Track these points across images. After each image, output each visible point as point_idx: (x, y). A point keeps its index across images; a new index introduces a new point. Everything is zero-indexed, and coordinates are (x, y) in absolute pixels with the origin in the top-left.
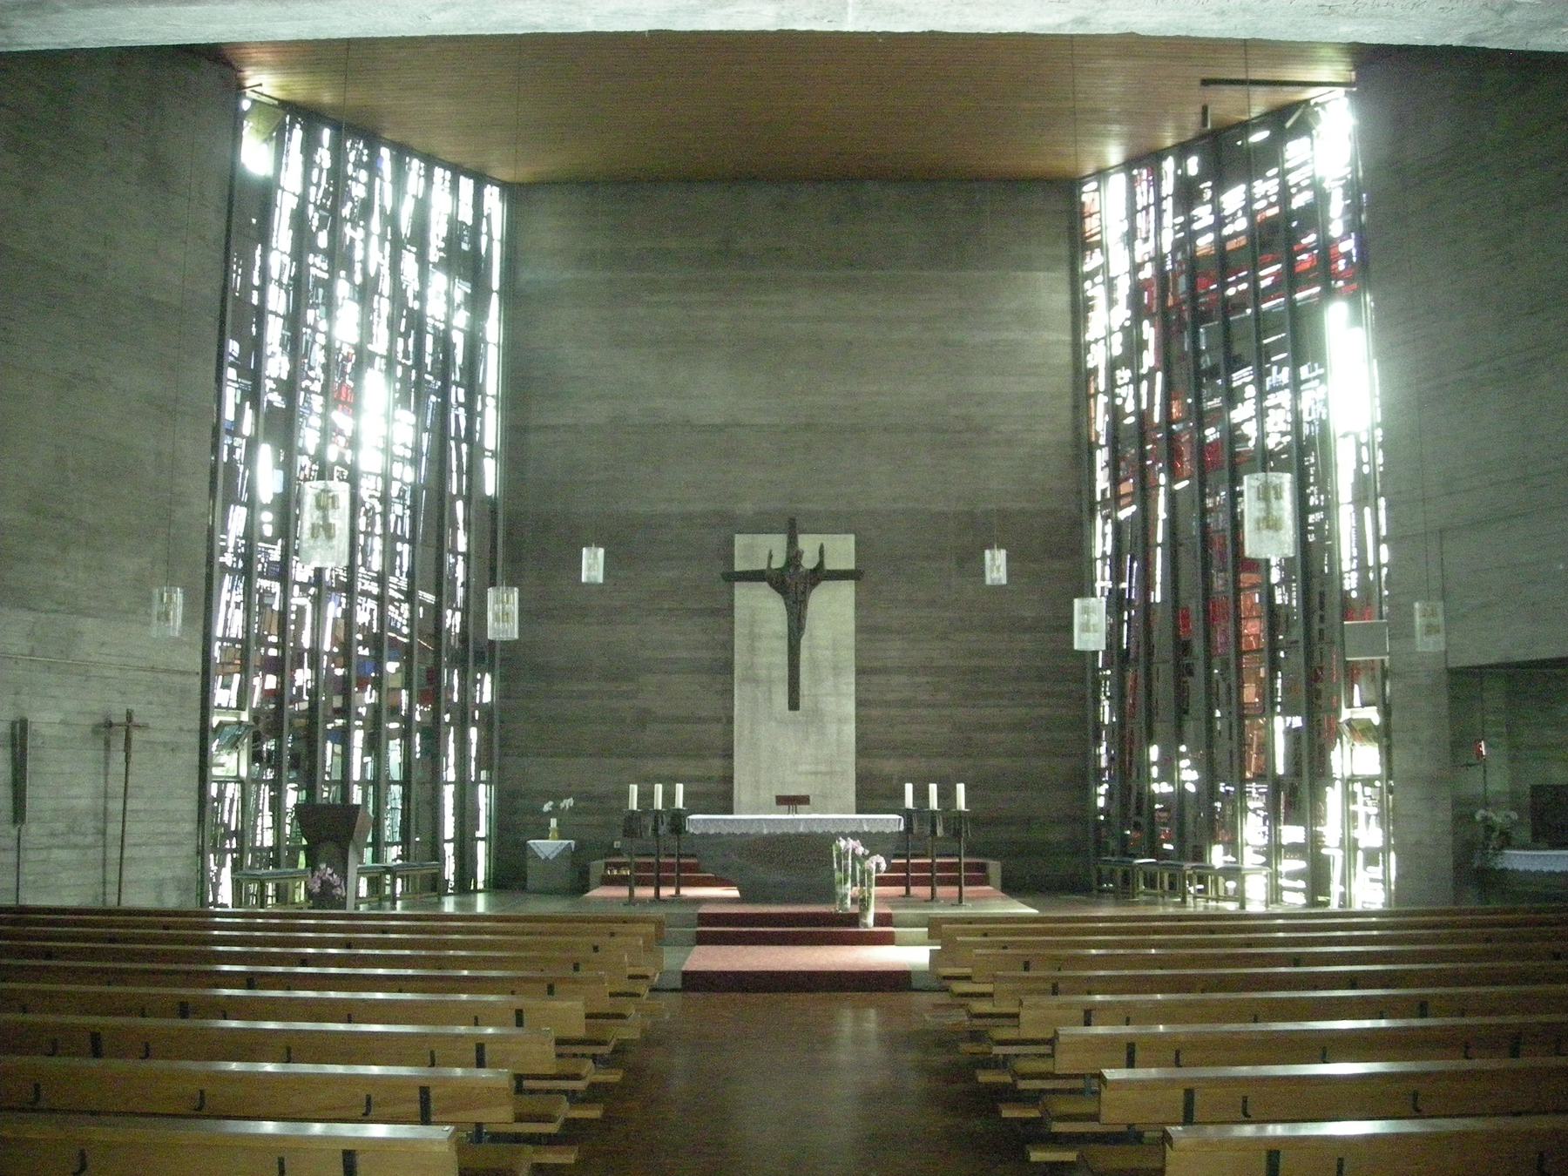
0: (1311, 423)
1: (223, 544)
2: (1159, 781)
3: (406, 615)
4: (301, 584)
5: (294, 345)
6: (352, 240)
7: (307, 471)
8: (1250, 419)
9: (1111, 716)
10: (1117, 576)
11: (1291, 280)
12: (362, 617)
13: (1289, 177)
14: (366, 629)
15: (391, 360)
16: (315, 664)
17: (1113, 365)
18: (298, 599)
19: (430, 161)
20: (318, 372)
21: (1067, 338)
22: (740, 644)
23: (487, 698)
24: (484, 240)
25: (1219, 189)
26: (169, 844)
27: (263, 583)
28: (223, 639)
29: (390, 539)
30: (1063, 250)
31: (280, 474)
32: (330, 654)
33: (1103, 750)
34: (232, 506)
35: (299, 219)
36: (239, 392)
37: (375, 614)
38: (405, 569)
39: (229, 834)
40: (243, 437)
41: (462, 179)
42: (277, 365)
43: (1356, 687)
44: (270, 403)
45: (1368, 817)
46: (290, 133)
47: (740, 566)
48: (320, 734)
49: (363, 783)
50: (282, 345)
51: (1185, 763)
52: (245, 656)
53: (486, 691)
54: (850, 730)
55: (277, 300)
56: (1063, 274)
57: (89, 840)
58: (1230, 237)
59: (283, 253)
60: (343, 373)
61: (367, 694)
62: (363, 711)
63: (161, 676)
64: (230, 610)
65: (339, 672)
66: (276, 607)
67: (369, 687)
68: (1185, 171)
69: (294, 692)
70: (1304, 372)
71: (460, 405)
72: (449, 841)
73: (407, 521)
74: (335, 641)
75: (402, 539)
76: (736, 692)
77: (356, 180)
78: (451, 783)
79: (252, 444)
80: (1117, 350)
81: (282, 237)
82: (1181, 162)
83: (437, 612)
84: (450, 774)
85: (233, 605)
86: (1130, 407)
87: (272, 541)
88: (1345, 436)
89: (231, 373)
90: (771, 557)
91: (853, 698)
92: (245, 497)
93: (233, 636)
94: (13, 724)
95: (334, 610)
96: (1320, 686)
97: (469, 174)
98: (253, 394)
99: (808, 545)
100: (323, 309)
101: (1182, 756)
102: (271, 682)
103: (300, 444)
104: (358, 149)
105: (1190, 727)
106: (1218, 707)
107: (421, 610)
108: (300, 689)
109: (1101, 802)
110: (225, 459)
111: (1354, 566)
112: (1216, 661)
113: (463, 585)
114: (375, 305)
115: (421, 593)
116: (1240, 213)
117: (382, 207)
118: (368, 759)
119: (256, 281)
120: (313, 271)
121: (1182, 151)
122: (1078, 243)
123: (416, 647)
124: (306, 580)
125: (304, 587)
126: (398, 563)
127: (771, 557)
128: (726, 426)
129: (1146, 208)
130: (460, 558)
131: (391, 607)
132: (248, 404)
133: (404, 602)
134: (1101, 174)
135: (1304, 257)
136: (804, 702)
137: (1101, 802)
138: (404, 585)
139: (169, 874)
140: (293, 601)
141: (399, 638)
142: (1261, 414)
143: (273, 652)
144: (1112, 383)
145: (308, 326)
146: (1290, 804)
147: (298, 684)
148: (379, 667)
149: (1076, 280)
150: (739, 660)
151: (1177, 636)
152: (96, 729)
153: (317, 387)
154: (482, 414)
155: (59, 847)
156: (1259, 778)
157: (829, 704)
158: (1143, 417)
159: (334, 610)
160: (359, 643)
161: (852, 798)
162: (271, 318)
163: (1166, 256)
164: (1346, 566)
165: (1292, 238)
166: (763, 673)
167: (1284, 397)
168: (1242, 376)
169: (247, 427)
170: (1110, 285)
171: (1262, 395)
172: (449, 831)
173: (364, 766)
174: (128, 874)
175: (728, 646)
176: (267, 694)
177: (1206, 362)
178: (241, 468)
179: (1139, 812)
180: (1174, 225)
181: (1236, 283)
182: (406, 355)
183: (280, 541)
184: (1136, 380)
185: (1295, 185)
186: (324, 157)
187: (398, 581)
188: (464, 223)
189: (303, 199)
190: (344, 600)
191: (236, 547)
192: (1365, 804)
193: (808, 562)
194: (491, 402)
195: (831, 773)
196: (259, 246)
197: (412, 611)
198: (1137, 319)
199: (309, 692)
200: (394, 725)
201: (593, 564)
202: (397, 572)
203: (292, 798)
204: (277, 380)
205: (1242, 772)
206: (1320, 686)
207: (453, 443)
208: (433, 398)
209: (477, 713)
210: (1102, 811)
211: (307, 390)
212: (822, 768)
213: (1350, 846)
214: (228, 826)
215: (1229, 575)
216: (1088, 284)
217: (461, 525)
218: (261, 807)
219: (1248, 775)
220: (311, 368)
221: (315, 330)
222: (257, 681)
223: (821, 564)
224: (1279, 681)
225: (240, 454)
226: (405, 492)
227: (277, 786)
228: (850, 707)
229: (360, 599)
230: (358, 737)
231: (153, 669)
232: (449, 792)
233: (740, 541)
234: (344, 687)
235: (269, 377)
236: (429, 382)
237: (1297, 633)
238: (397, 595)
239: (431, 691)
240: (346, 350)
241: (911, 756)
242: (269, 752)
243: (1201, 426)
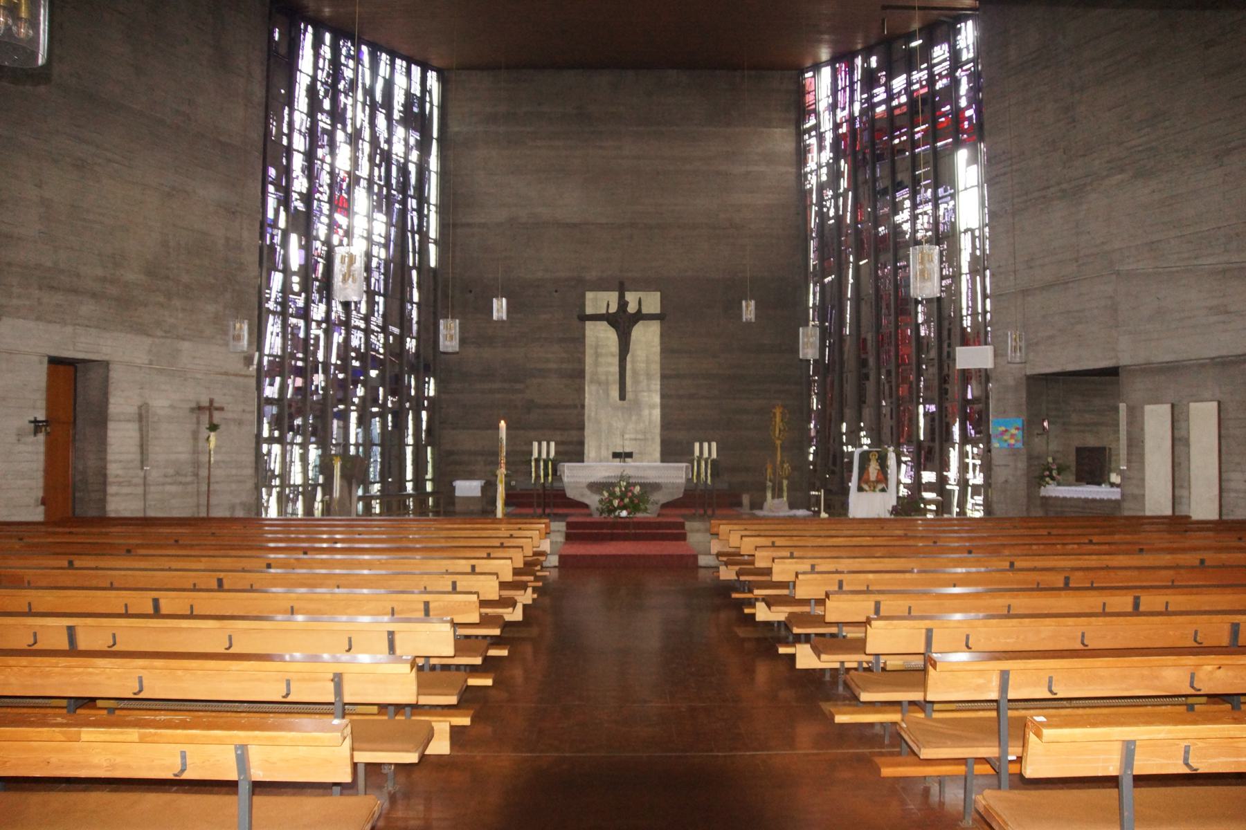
0: (944, 224)
1: (267, 296)
2: (847, 445)
3: (382, 341)
4: (317, 321)
5: (311, 172)
6: (345, 105)
7: (319, 251)
8: (907, 221)
9: (817, 406)
10: (822, 320)
11: (934, 134)
12: (355, 342)
13: (935, 69)
14: (357, 350)
15: (370, 181)
16: (326, 372)
17: (821, 187)
18: (315, 331)
19: (393, 55)
20: (326, 189)
21: (793, 170)
22: (589, 360)
23: (432, 393)
24: (428, 106)
25: (891, 77)
26: (240, 482)
27: (293, 321)
28: (269, 355)
29: (371, 294)
30: (793, 115)
31: (303, 252)
32: (335, 365)
33: (812, 426)
35: (312, 91)
37: (363, 340)
38: (381, 312)
39: (275, 477)
40: (279, 229)
41: (414, 67)
42: (300, 184)
43: (969, 386)
45: (974, 466)
46: (304, 35)
47: (589, 310)
48: (330, 414)
49: (357, 445)
50: (303, 171)
51: (863, 434)
52: (280, 367)
53: (431, 390)
54: (657, 413)
55: (299, 143)
56: (792, 130)
57: (189, 479)
58: (896, 107)
59: (302, 112)
60: (341, 189)
61: (358, 390)
62: (356, 400)
63: (232, 378)
65: (341, 376)
66: (302, 335)
67: (359, 385)
68: (869, 64)
69: (313, 388)
70: (941, 191)
71: (413, 210)
72: (409, 481)
73: (382, 283)
74: (338, 358)
75: (379, 294)
77: (347, 66)
80: (824, 178)
81: (302, 102)
82: (866, 60)
83: (401, 340)
84: (410, 440)
86: (832, 213)
87: (299, 294)
88: (966, 231)
89: (271, 188)
90: (608, 305)
91: (659, 393)
92: (281, 267)
93: (275, 353)
94: (140, 407)
95: (338, 338)
96: (947, 386)
97: (417, 64)
98: (285, 201)
99: (631, 298)
101: (861, 429)
102: (299, 382)
103: (314, 233)
104: (347, 46)
105: (867, 412)
106: (884, 399)
107: (391, 338)
108: (317, 386)
109: (811, 458)
110: (268, 242)
111: (969, 313)
112: (883, 371)
114: (360, 146)
115: (390, 327)
116: (903, 92)
117: (364, 84)
118: (359, 430)
119: (285, 130)
120: (321, 124)
121: (867, 53)
122: (800, 109)
123: (388, 362)
124: (319, 319)
125: (319, 323)
126: (376, 308)
127: (608, 305)
128: (580, 224)
129: (844, 89)
130: (415, 306)
131: (372, 336)
132: (282, 208)
134: (817, 67)
135: (943, 119)
136: (629, 395)
137: (811, 458)
138: (380, 323)
139: (238, 501)
140: (312, 332)
141: (377, 355)
142: (914, 218)
143: (300, 364)
144: (821, 198)
145: (319, 160)
146: (927, 459)
147: (315, 383)
148: (366, 374)
149: (800, 134)
150: (588, 369)
151: (859, 356)
152: (192, 410)
153: (325, 198)
154: (428, 216)
155: (171, 484)
156: (909, 442)
157: (644, 397)
158: (839, 219)
159: (338, 338)
160: (353, 358)
161: (657, 455)
162: (295, 153)
163: (856, 118)
164: (964, 312)
165: (936, 108)
166: (603, 378)
167: (928, 208)
168: (903, 195)
169: (282, 223)
170: (821, 137)
171: (914, 206)
172: (409, 475)
173: (357, 434)
174: (214, 500)
175: (582, 361)
176: (297, 390)
177: (880, 185)
179: (834, 464)
180: (861, 99)
181: (899, 137)
182: (380, 179)
183: (303, 295)
184: (836, 197)
185: (938, 74)
186: (326, 51)
187: (377, 320)
188: (416, 95)
189: (314, 79)
190: (343, 332)
191: (276, 298)
192: (973, 458)
193: (632, 308)
194: (433, 208)
195: (645, 440)
197: (386, 339)
198: (836, 159)
199: (323, 389)
200: (375, 410)
201: (500, 308)
202: (376, 314)
204: (300, 194)
205: (899, 439)
206: (947, 386)
207: (409, 234)
208: (397, 206)
209: (426, 403)
210: (811, 463)
211: (319, 200)
212: (640, 436)
213: (963, 483)
214: (274, 471)
215: (892, 318)
216: (806, 137)
217: (415, 285)
219: (901, 440)
220: (321, 186)
221: (323, 161)
222: (290, 381)
223: (639, 310)
224: (922, 383)
225: (277, 240)
226: (380, 264)
227: (304, 446)
228: (657, 399)
229: (354, 331)
230: (354, 416)
231: (226, 374)
232: (409, 450)
233: (589, 295)
234: (342, 385)
235: (295, 192)
236: (394, 195)
237: (933, 354)
238: (376, 329)
239: (396, 387)
240: (342, 174)
242: (298, 426)
243: (876, 226)
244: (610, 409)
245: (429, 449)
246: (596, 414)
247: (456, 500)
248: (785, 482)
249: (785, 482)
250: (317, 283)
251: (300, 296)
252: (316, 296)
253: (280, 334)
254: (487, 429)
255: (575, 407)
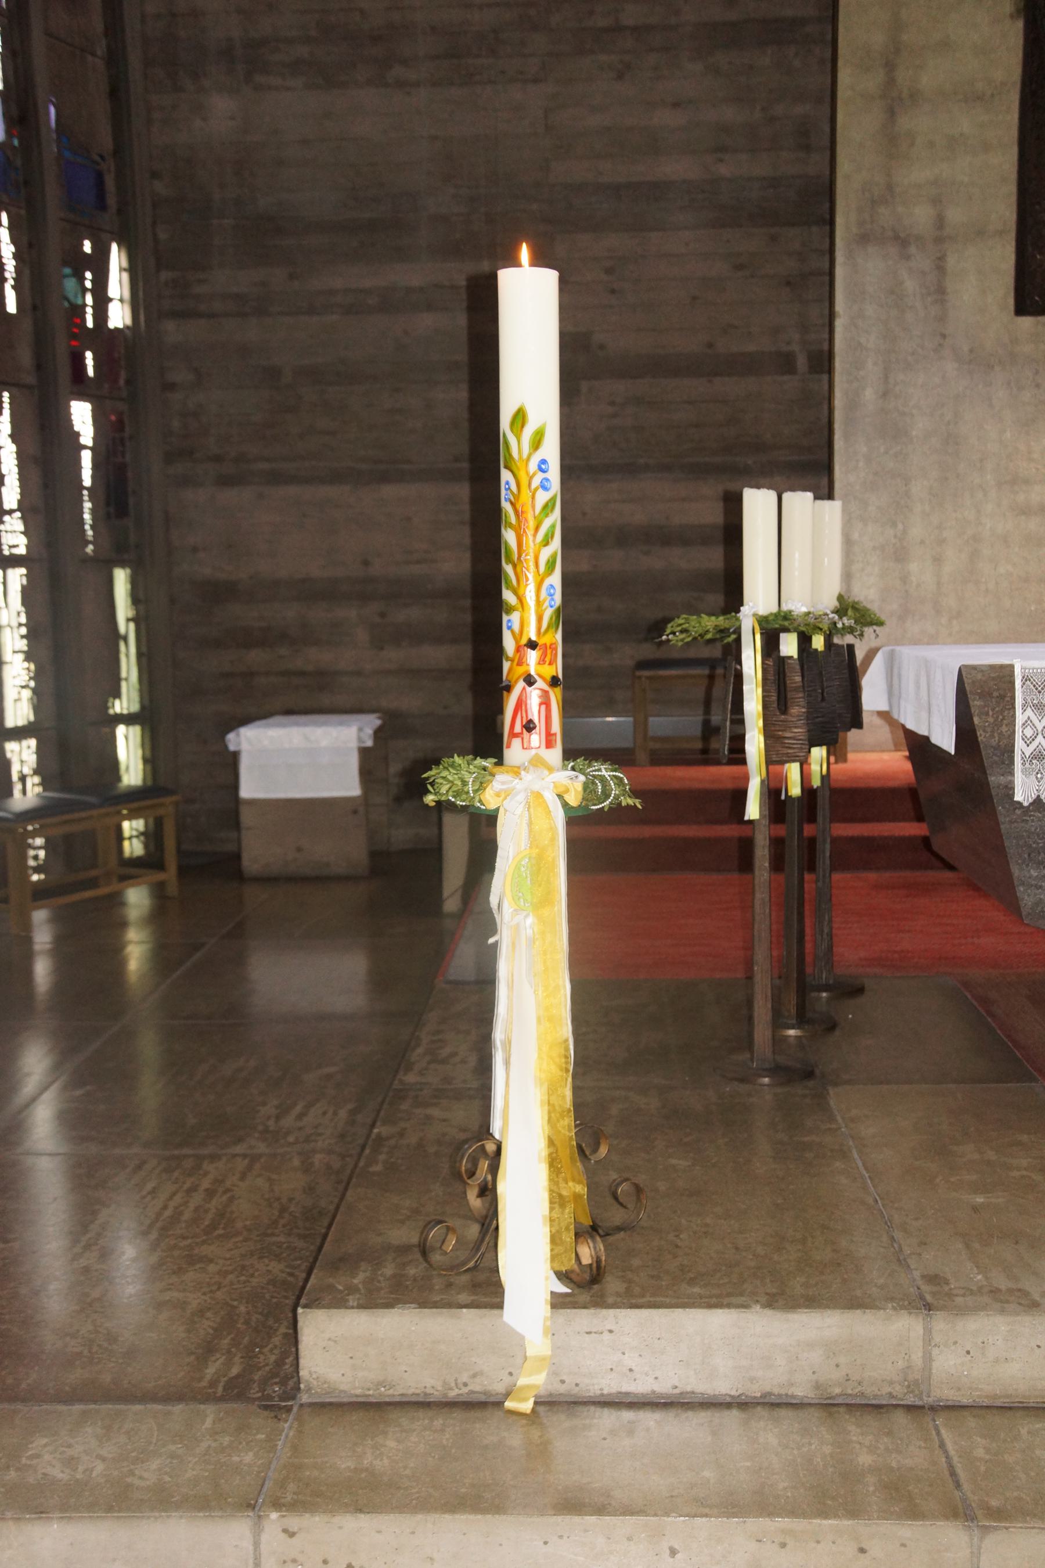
23: (118, 316)
72: (19, 734)
76: (840, 272)
166: (921, 216)
244: (950, 367)
245: (121, 579)
246: (885, 395)
247: (247, 817)
254: (384, 478)
255: (786, 363)
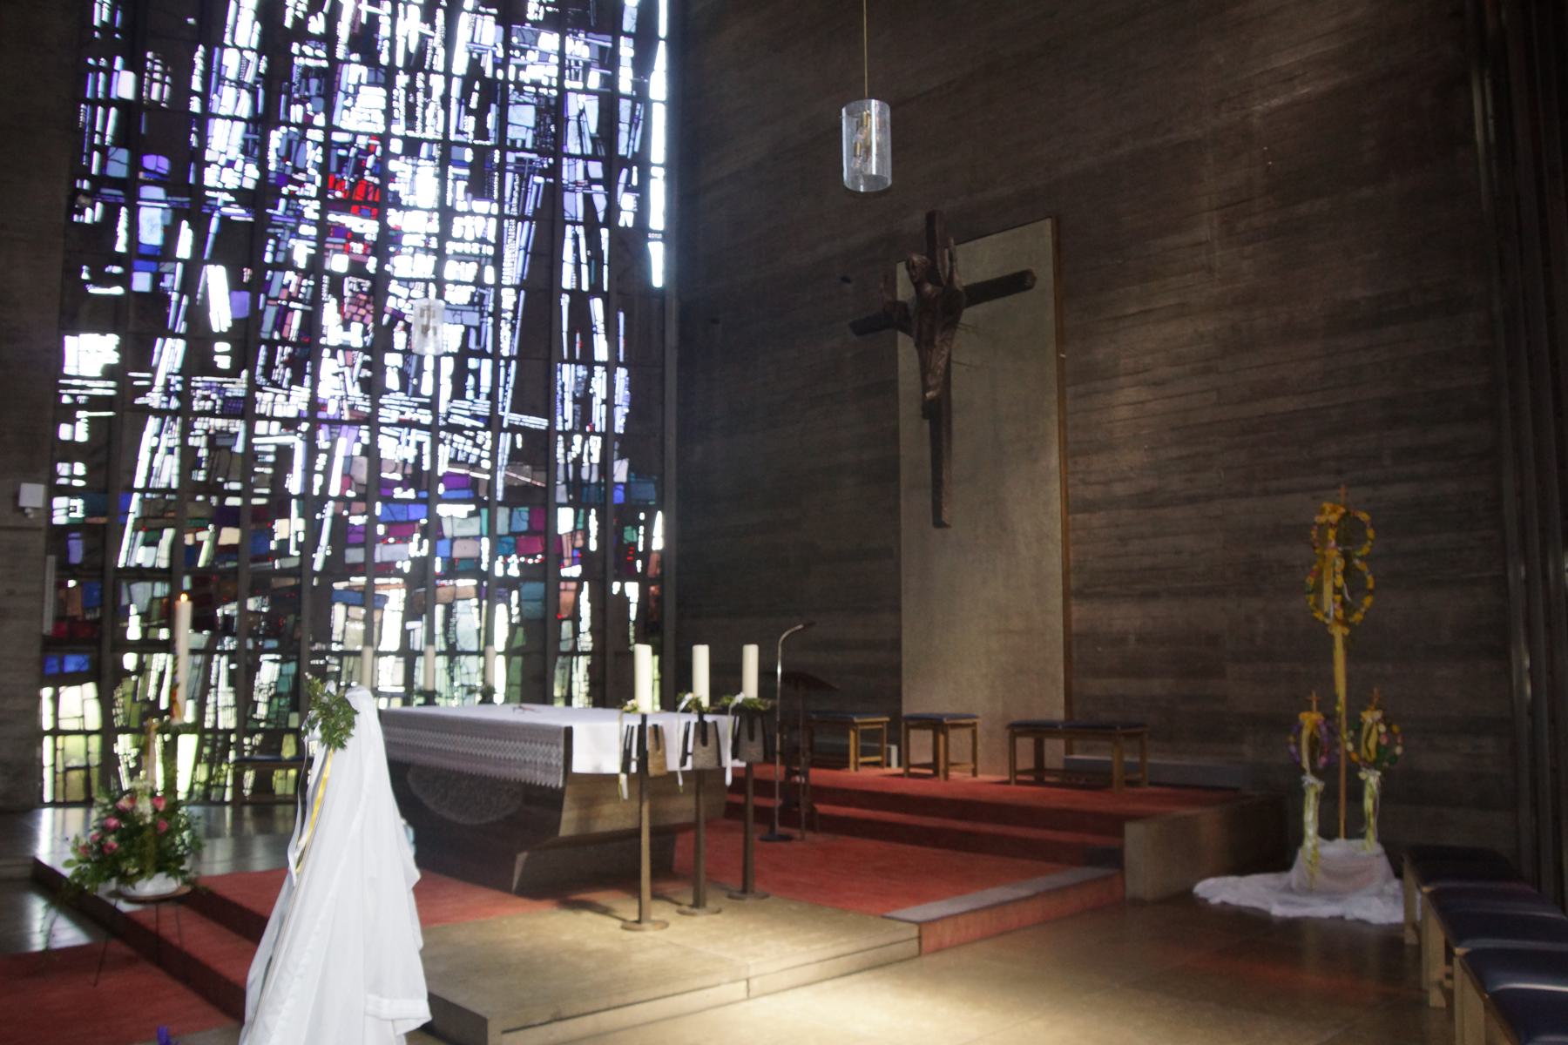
7: (292, 289)
23: (658, 544)
28: (143, 491)
34: (159, 341)
36: (170, 211)
44: (225, 220)
64: (158, 457)
69: (273, 546)
75: (481, 354)
78: (584, 653)
79: (193, 270)
84: (586, 642)
85: (162, 450)
87: (234, 373)
100: (321, 102)
102: (230, 536)
113: (604, 402)
119: (196, 85)
120: (299, 61)
124: (292, 414)
132: (185, 224)
133: (484, 430)
143: (233, 501)
147: (277, 537)
153: (312, 190)
178: (175, 296)
191: (168, 384)
196: (201, 48)
199: (299, 546)
202: (470, 394)
203: (268, 671)
211: (292, 196)
218: (213, 682)
226: (482, 297)
241: (1155, 595)
248: (1372, 779)
249: (1372, 779)
250: (288, 350)
251: (238, 376)
252: (283, 374)
253: (177, 450)
